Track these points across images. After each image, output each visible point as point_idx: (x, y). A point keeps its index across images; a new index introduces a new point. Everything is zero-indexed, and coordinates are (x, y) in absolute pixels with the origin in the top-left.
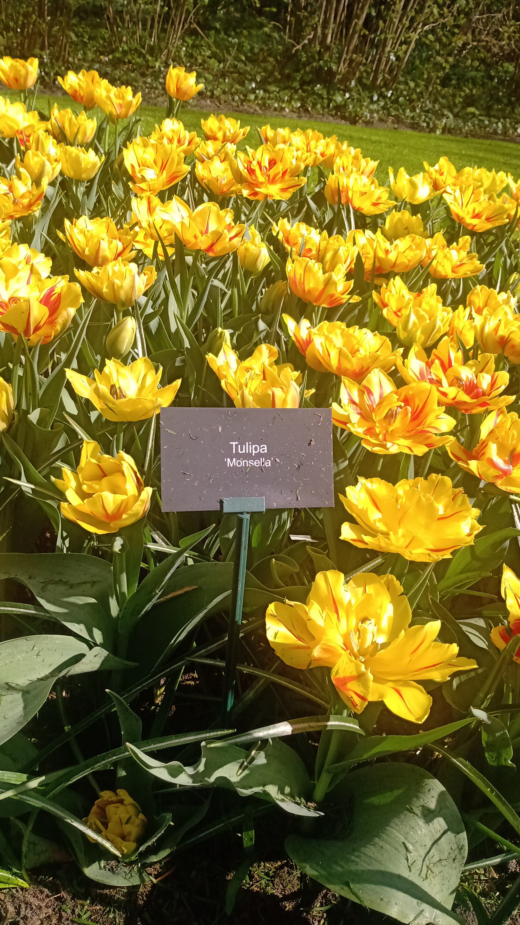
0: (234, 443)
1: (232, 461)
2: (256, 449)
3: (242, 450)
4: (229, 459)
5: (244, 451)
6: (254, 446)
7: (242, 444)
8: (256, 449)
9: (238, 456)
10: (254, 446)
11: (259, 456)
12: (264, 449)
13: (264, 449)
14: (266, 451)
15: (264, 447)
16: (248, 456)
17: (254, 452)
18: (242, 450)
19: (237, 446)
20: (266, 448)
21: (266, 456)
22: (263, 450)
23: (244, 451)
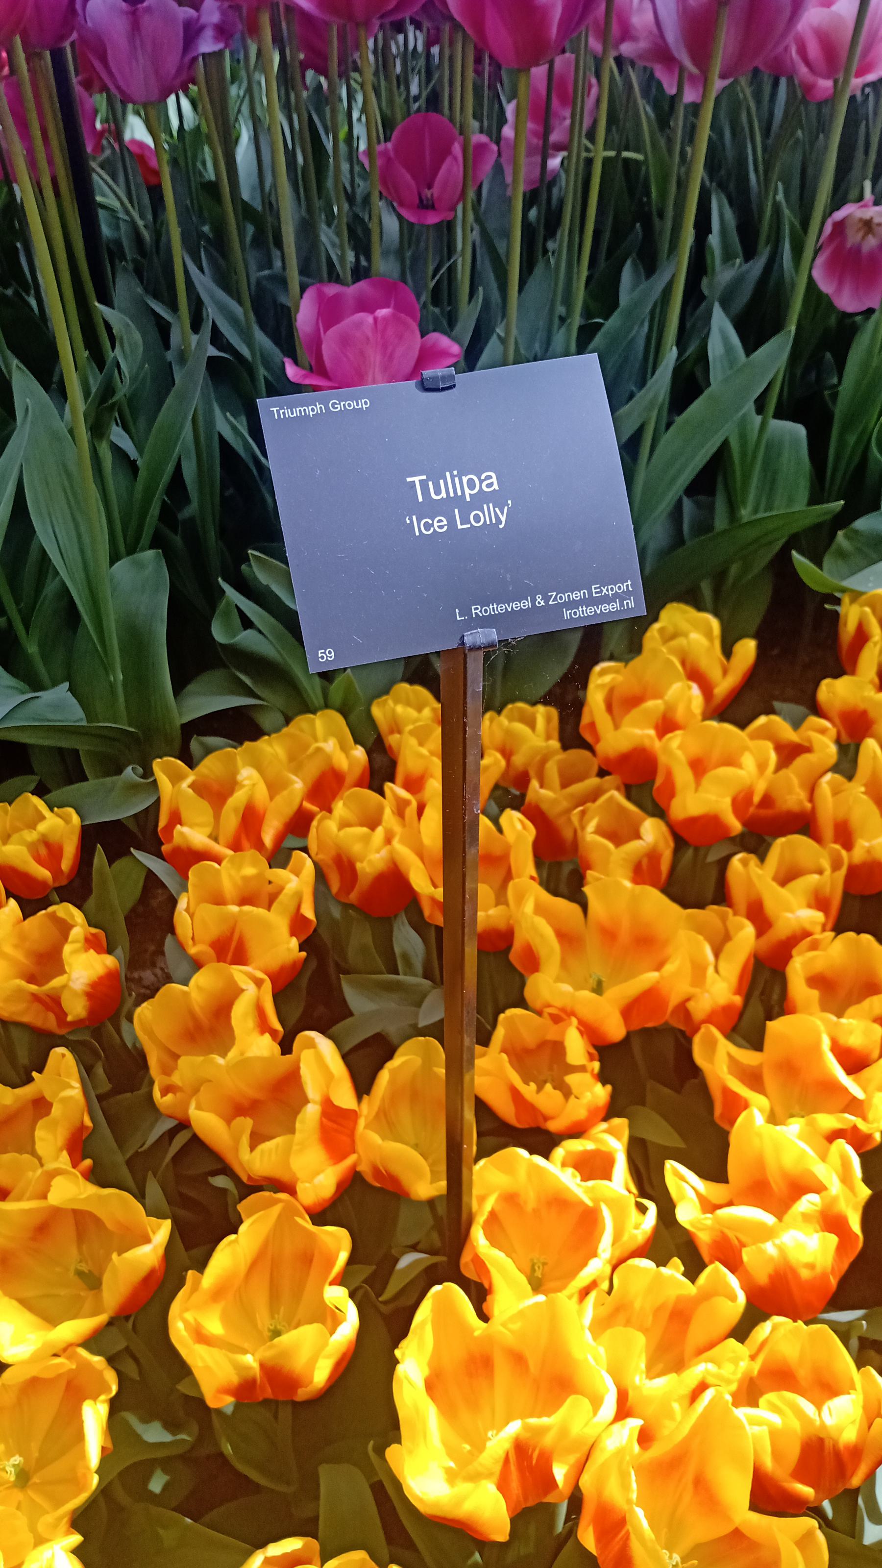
0: (416, 479)
3: (438, 492)
5: (443, 495)
6: (465, 479)
7: (436, 476)
9: (431, 509)
10: (465, 479)
11: (480, 499)
12: (491, 482)
13: (491, 482)
14: (496, 487)
15: (490, 477)
17: (467, 491)
18: (438, 492)
20: (494, 480)
21: (498, 499)
22: (490, 485)
23: (443, 495)
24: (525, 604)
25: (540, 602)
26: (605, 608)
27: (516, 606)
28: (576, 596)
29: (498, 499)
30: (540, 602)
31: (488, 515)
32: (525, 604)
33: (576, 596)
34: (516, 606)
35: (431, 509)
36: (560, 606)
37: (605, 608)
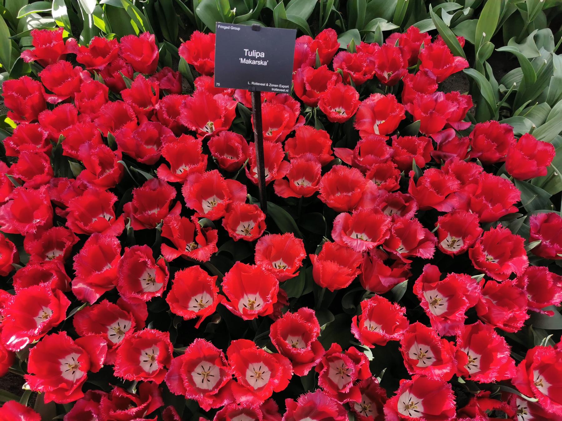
0: (246, 50)
2: (258, 54)
7: (251, 51)
8: (258, 54)
11: (259, 59)
12: (263, 55)
13: (263, 55)
16: (253, 58)
24: (264, 85)
25: (267, 85)
26: (281, 90)
27: (262, 84)
28: (276, 86)
30: (267, 85)
31: (261, 63)
32: (264, 85)
33: (276, 86)
34: (262, 84)
36: (272, 87)
37: (281, 90)
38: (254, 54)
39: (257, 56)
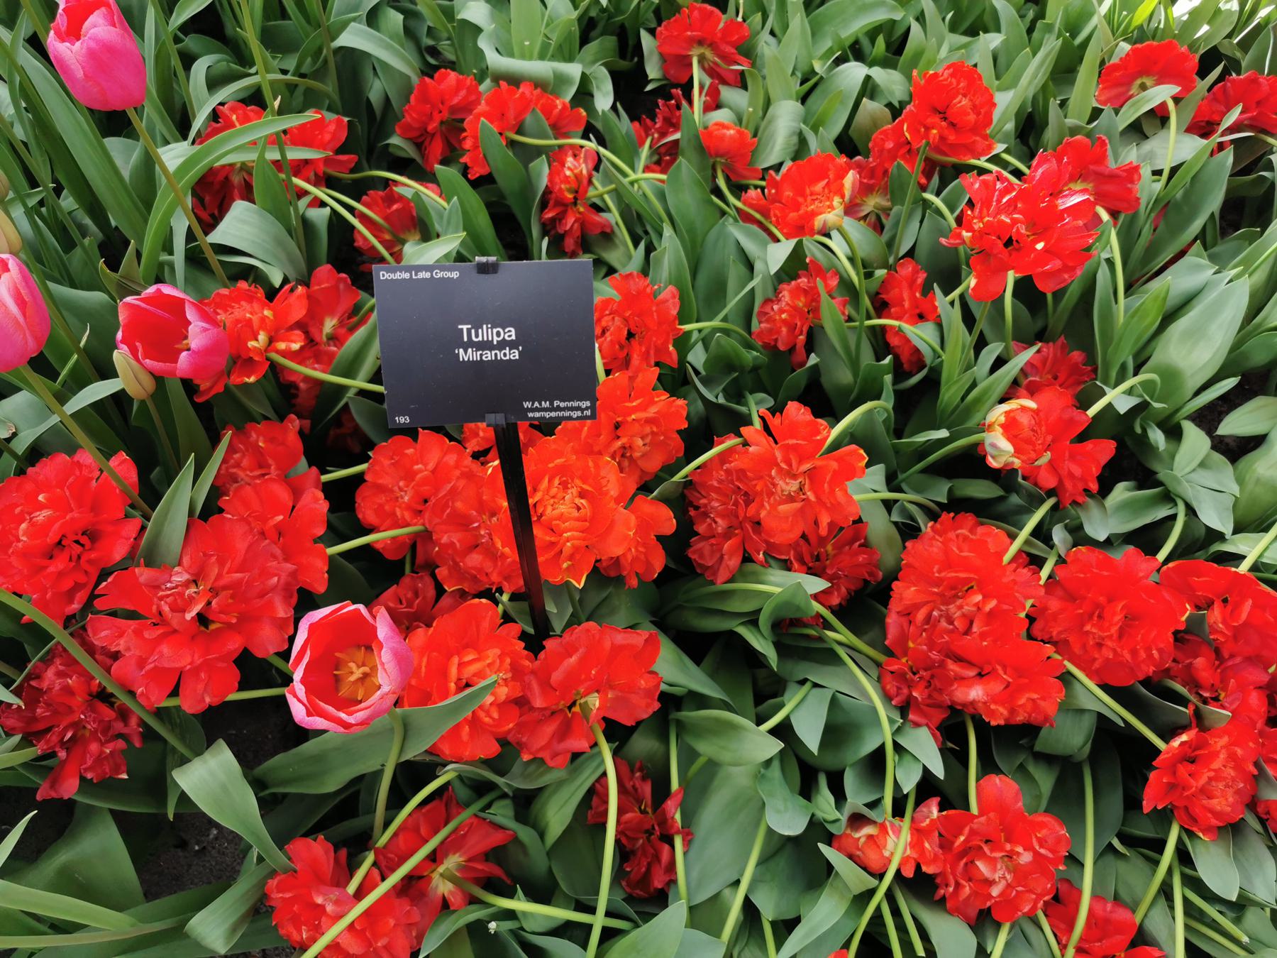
0: (465, 327)
1: (466, 352)
2: (498, 334)
3: (477, 336)
4: (461, 351)
5: (480, 338)
7: (477, 327)
8: (498, 334)
11: (502, 345)
12: (510, 334)
13: (510, 334)
14: (513, 337)
16: (486, 345)
17: (496, 339)
18: (477, 336)
19: (469, 331)
20: (513, 333)
21: (512, 345)
29: (512, 345)
35: (470, 344)
38: (488, 333)
39: (496, 339)
